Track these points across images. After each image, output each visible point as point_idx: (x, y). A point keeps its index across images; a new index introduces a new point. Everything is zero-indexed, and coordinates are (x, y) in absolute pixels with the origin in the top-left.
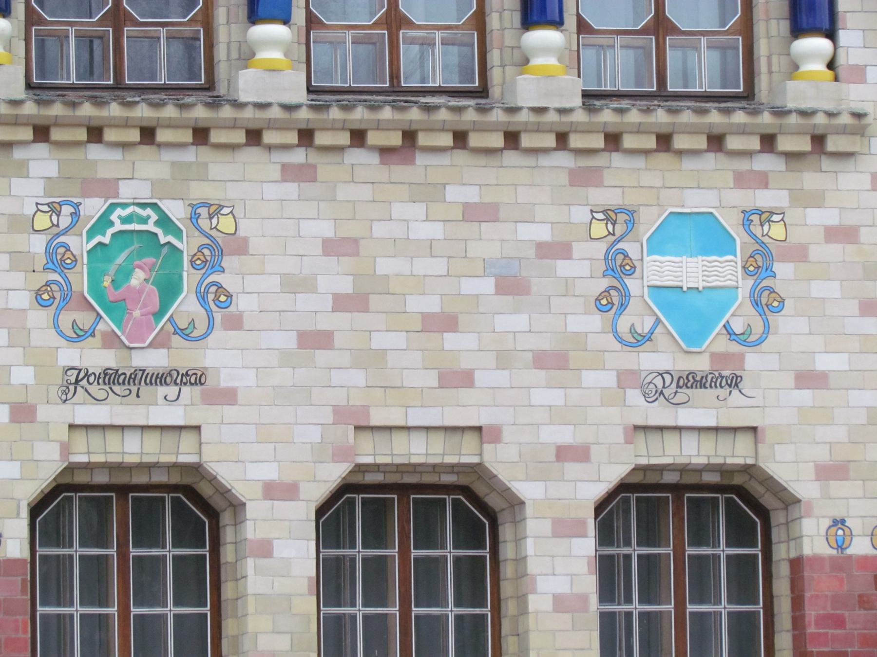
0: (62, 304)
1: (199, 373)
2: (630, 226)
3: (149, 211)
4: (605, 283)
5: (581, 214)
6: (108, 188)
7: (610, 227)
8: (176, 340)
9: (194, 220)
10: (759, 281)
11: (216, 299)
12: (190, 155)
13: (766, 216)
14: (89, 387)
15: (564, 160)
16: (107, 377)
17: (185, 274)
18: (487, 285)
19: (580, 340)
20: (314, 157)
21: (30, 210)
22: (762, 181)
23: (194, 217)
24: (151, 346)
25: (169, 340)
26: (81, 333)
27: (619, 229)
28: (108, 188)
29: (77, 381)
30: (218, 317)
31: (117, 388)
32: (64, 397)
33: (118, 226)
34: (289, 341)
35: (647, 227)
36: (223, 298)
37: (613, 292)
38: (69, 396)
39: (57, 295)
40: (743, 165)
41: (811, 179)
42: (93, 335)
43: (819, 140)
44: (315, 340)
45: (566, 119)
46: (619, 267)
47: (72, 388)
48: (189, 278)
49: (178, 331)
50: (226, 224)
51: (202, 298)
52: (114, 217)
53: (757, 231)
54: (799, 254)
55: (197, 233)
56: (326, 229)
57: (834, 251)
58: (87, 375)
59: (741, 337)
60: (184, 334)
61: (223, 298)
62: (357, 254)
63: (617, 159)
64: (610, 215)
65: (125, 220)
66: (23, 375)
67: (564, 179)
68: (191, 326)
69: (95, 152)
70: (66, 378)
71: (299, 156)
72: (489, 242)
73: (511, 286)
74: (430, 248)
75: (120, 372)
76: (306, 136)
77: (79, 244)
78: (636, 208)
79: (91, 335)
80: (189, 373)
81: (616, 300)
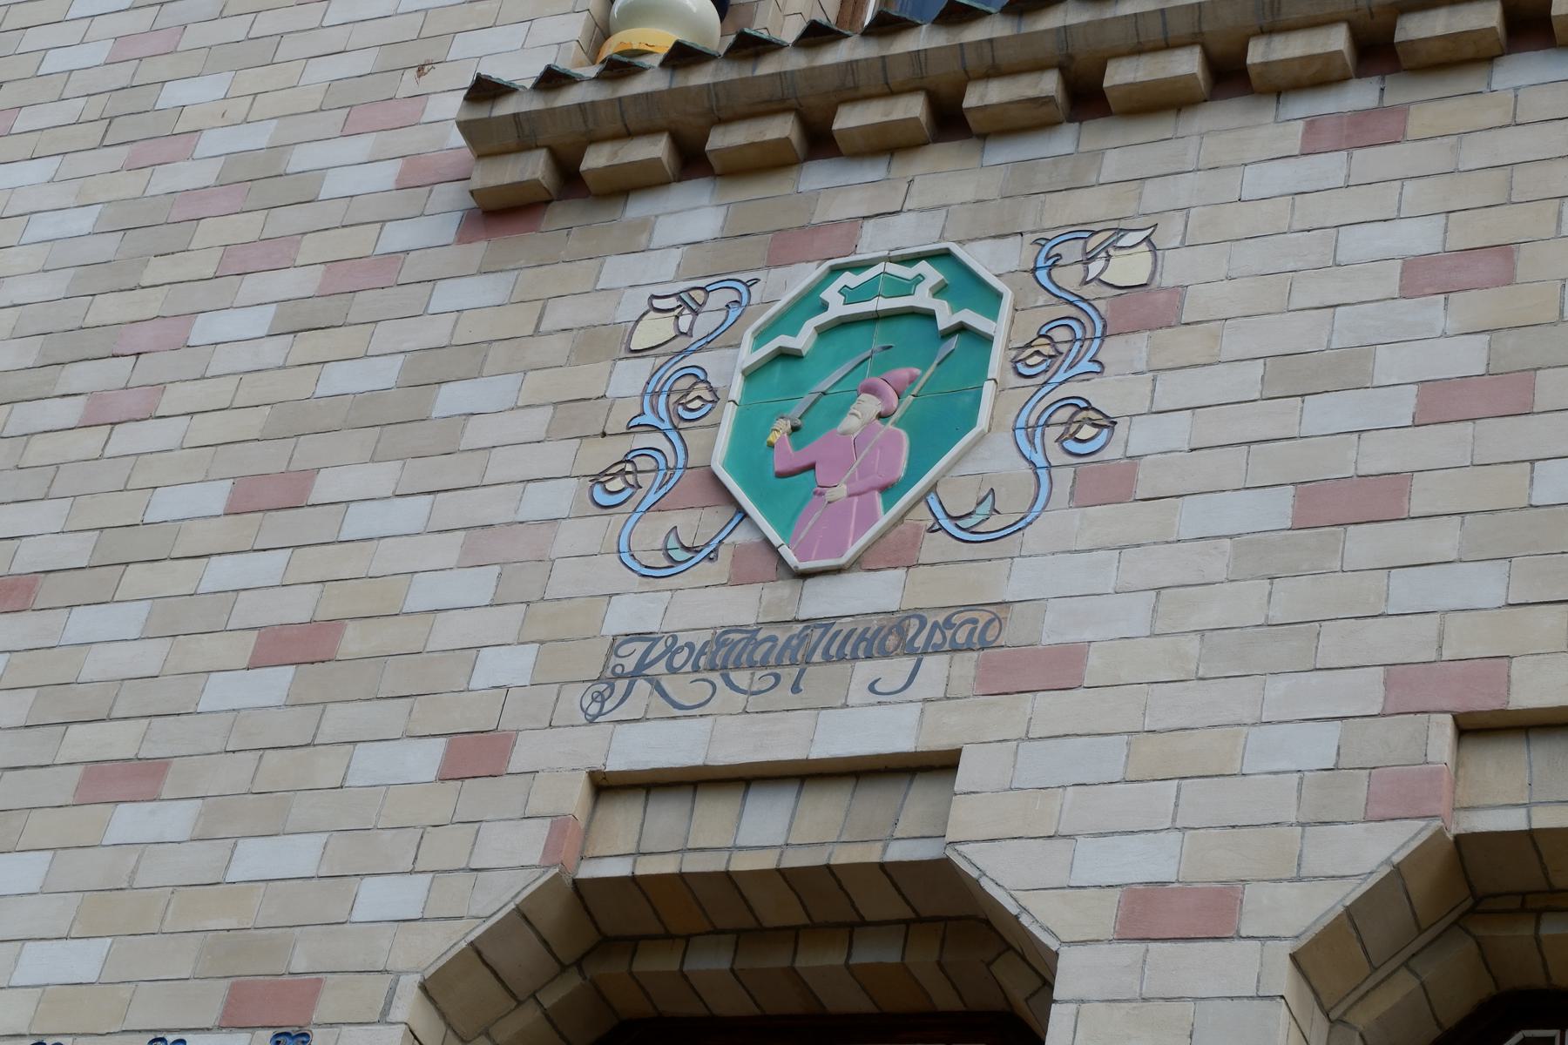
0: (651, 498)
1: (983, 617)
3: (923, 267)
9: (1042, 275)
14: (666, 683)
16: (723, 651)
17: (988, 389)
25: (916, 545)
26: (679, 555)
29: (641, 666)
31: (741, 678)
32: (594, 709)
33: (838, 308)
34: (1277, 509)
36: (1086, 432)
38: (608, 705)
44: (1344, 504)
47: (622, 685)
48: (998, 398)
49: (946, 523)
50: (1129, 267)
52: (831, 294)
55: (1043, 298)
58: (671, 651)
62: (1509, 281)
66: (510, 665)
68: (985, 509)
69: (817, 177)
70: (614, 661)
71: (1361, 95)
75: (760, 636)
79: (708, 558)
80: (956, 620)
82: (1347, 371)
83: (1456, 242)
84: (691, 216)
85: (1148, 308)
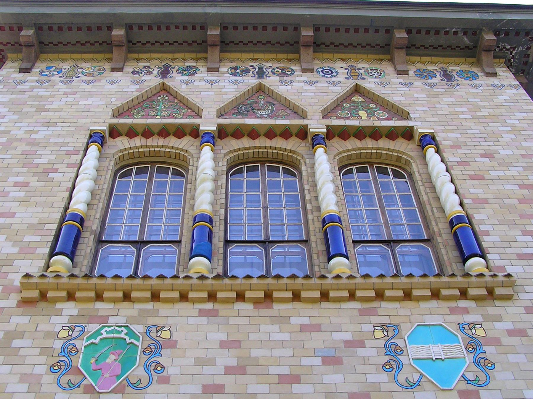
0: (64, 372)
2: (397, 332)
3: (123, 328)
4: (387, 358)
5: (368, 328)
6: (104, 320)
7: (385, 333)
8: (128, 389)
9: (148, 333)
10: (476, 355)
11: (156, 368)
12: (150, 306)
13: (472, 326)
15: (356, 305)
17: (138, 356)
18: (318, 361)
19: (376, 387)
20: (217, 306)
21: (58, 328)
22: (466, 311)
23: (148, 332)
24: (112, 392)
26: (72, 386)
27: (390, 334)
28: (104, 320)
30: (155, 378)
33: (105, 335)
34: (198, 389)
35: (406, 330)
36: (159, 368)
37: (392, 362)
39: (63, 367)
40: (453, 304)
41: (491, 310)
42: (79, 387)
43: (491, 292)
45: (352, 281)
46: (394, 351)
48: (140, 359)
50: (166, 334)
51: (147, 368)
52: (103, 331)
53: (470, 332)
54: (496, 342)
55: (148, 339)
56: (223, 337)
57: (515, 340)
59: (474, 382)
60: (134, 386)
61: (159, 368)
62: (240, 348)
63: (384, 304)
64: (384, 328)
65: (108, 333)
67: (356, 313)
68: (139, 382)
69: (99, 305)
71: (209, 306)
72: (316, 341)
73: (331, 361)
74: (283, 344)
76: (212, 297)
77: (81, 344)
78: (398, 324)
81: (394, 366)
82: (210, 362)
83: (230, 339)
84: (70, 309)
85: (172, 344)
